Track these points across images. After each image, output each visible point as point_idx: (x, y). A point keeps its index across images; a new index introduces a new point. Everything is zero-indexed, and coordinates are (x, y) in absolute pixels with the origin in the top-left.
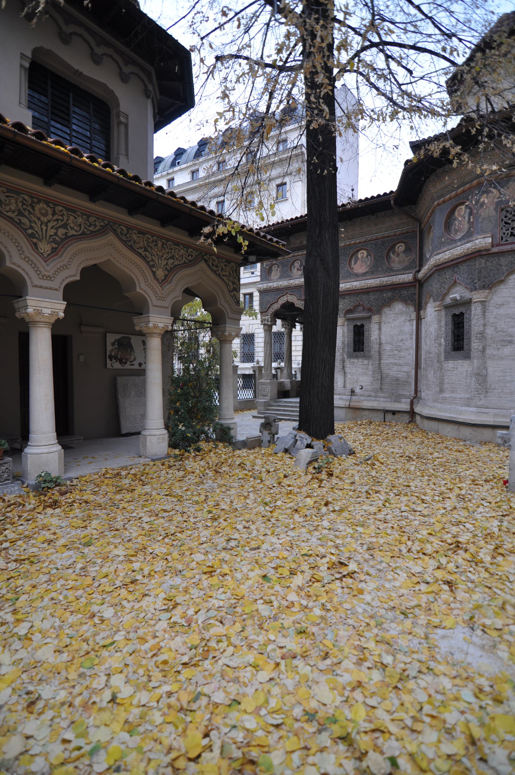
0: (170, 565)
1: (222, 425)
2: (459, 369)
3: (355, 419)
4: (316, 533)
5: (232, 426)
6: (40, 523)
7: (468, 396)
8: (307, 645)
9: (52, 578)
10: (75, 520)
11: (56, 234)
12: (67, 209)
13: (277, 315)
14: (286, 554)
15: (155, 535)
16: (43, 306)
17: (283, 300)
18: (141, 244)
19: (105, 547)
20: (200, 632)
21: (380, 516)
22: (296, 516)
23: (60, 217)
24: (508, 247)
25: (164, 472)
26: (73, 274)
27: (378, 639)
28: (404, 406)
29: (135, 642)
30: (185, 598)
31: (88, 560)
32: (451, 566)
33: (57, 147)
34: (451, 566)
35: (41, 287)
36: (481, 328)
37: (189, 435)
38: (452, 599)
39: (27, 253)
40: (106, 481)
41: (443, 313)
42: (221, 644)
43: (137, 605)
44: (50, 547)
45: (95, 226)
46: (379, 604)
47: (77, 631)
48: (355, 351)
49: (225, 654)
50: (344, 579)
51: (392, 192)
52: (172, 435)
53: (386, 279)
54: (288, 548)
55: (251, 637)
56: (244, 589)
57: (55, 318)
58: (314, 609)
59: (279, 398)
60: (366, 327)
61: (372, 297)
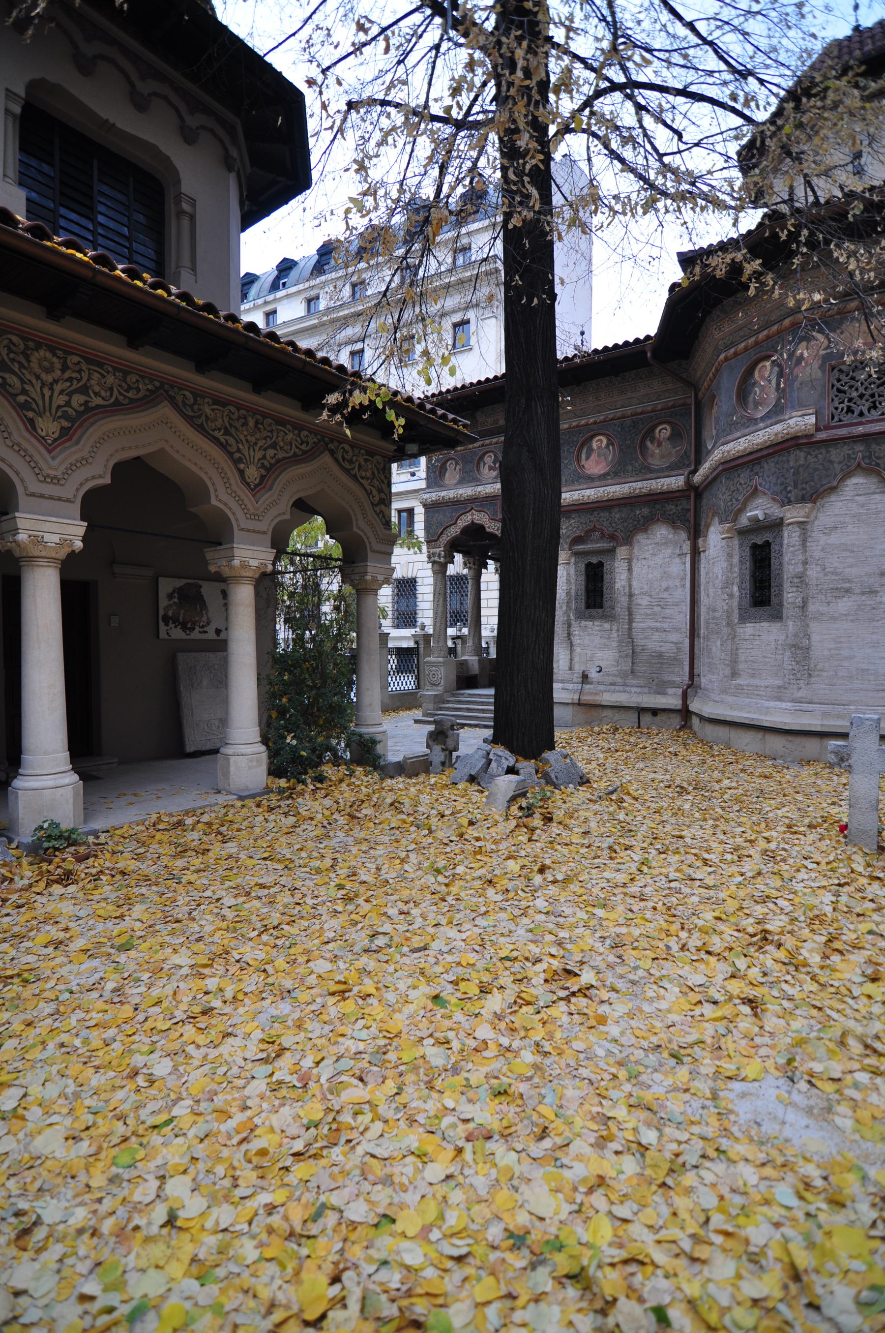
0: (270, 980)
1: (361, 735)
2: (764, 638)
3: (589, 723)
4: (525, 920)
5: (378, 737)
6: (40, 912)
7: (779, 682)
8: (510, 1115)
9: (62, 1009)
10: (103, 904)
11: (68, 404)
12: (89, 361)
13: (454, 546)
14: (472, 958)
15: (244, 929)
17: (464, 521)
18: (219, 423)
19: (156, 952)
20: (324, 1098)
21: (634, 889)
22: (490, 892)
23: (74, 375)
24: (843, 432)
25: (260, 818)
26: (98, 473)
27: (632, 1101)
28: (672, 700)
29: (209, 1118)
30: (297, 1039)
31: (126, 975)
32: (754, 973)
33: (70, 251)
34: (754, 973)
35: (42, 496)
36: (800, 568)
37: (304, 753)
38: (757, 1029)
39: (16, 436)
40: (159, 836)
41: (736, 542)
42: (360, 1118)
43: (213, 1053)
44: (59, 953)
45: (138, 390)
46: (633, 1040)
47: (106, 1101)
48: (588, 606)
49: (368, 1135)
50: (573, 1000)
51: (648, 337)
52: (274, 754)
53: (639, 485)
54: (477, 948)
55: (414, 1104)
56: (400, 1021)
57: (67, 550)
58: (523, 1052)
59: (459, 688)
60: (606, 567)
61: (616, 515)
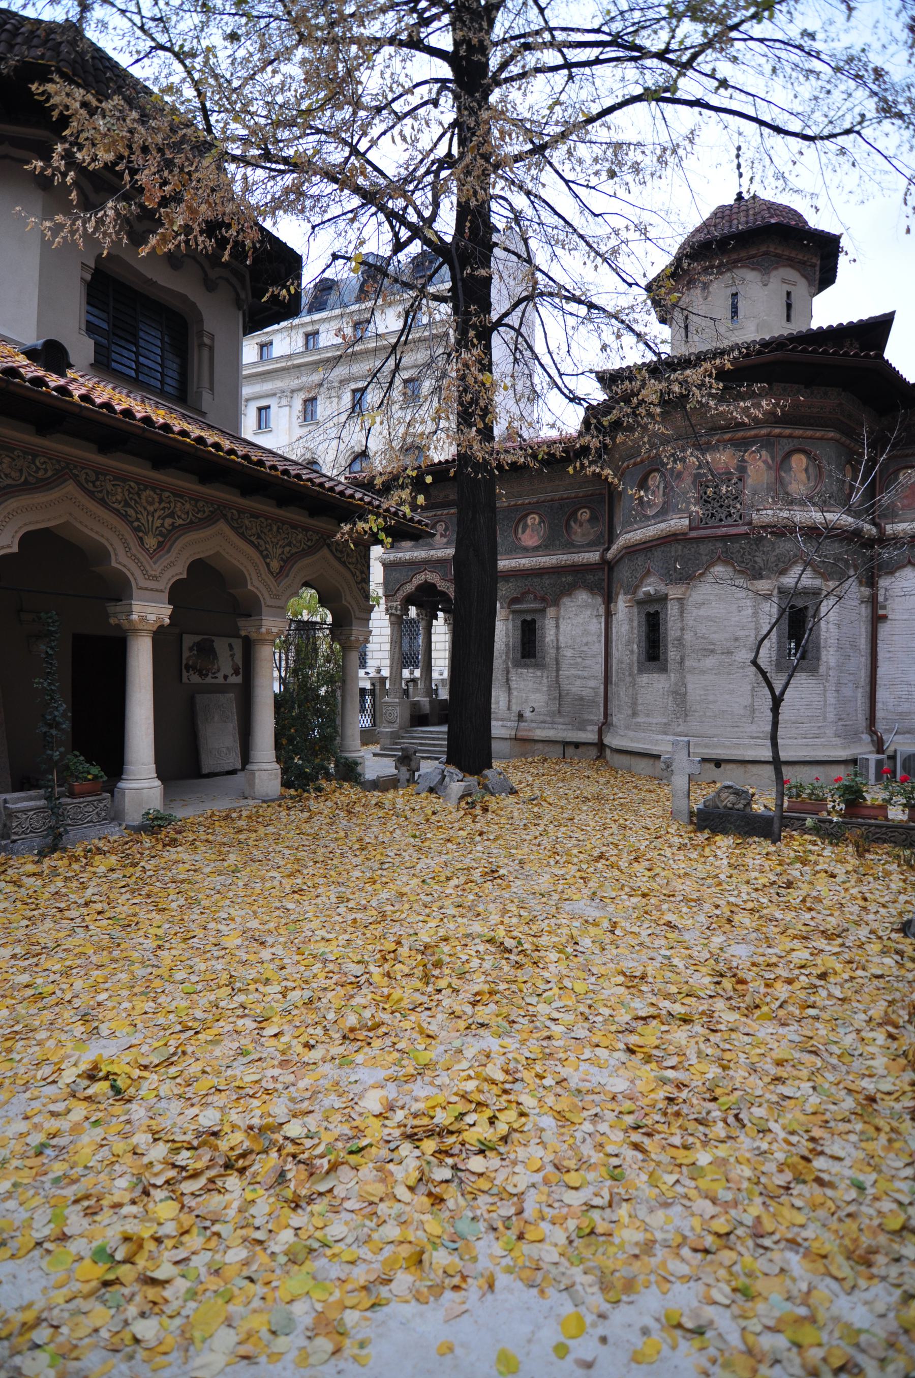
2: (654, 686)
3: (524, 755)
13: (409, 600)
16: (150, 611)
22: (449, 845)
24: (708, 532)
26: (179, 571)
28: (590, 736)
32: (591, 870)
39: (134, 551)
41: (635, 610)
48: (523, 656)
52: (284, 771)
53: (565, 557)
56: (405, 890)
60: (538, 624)
61: (547, 581)
